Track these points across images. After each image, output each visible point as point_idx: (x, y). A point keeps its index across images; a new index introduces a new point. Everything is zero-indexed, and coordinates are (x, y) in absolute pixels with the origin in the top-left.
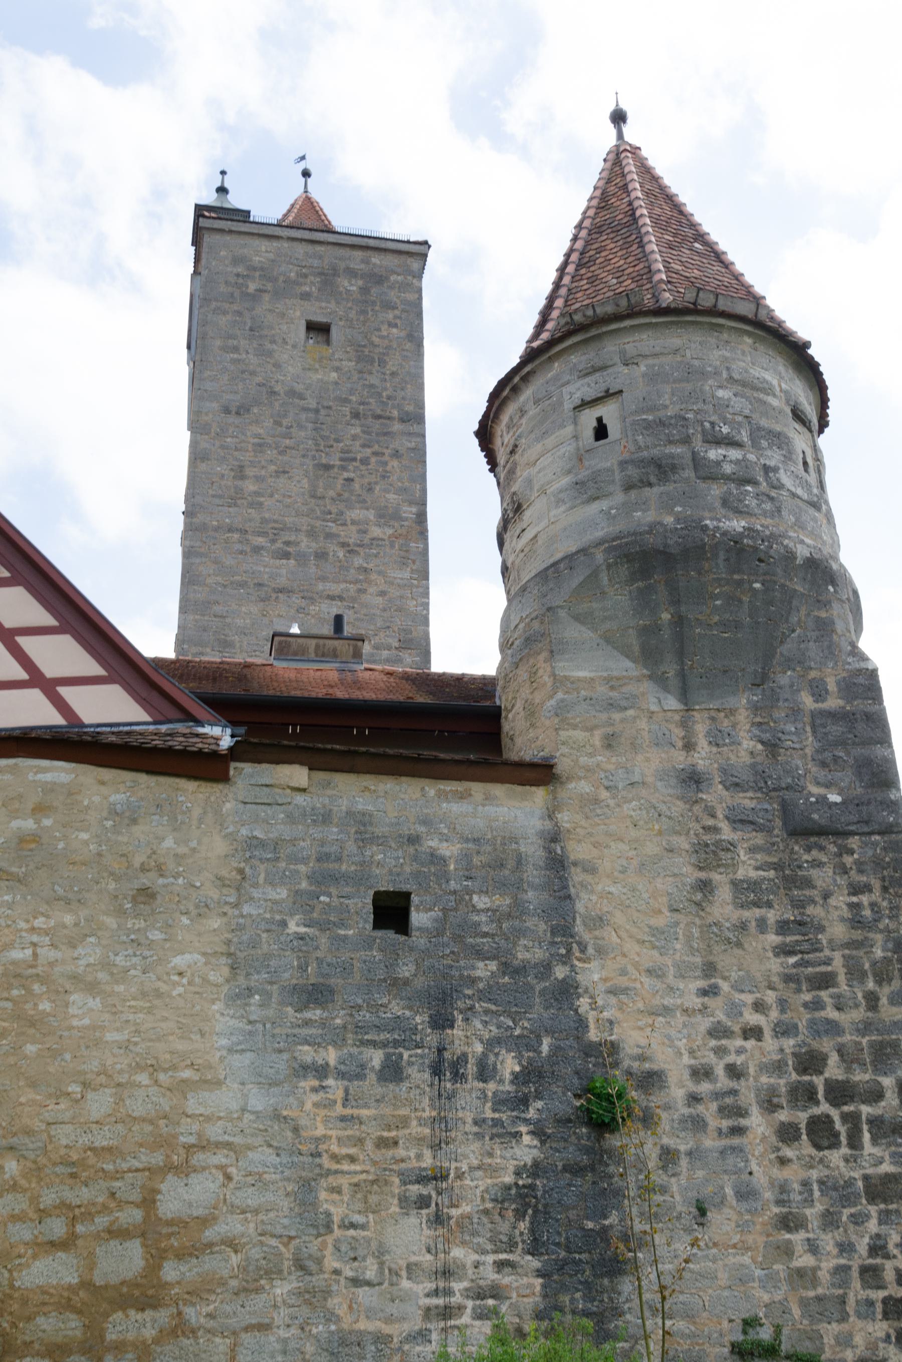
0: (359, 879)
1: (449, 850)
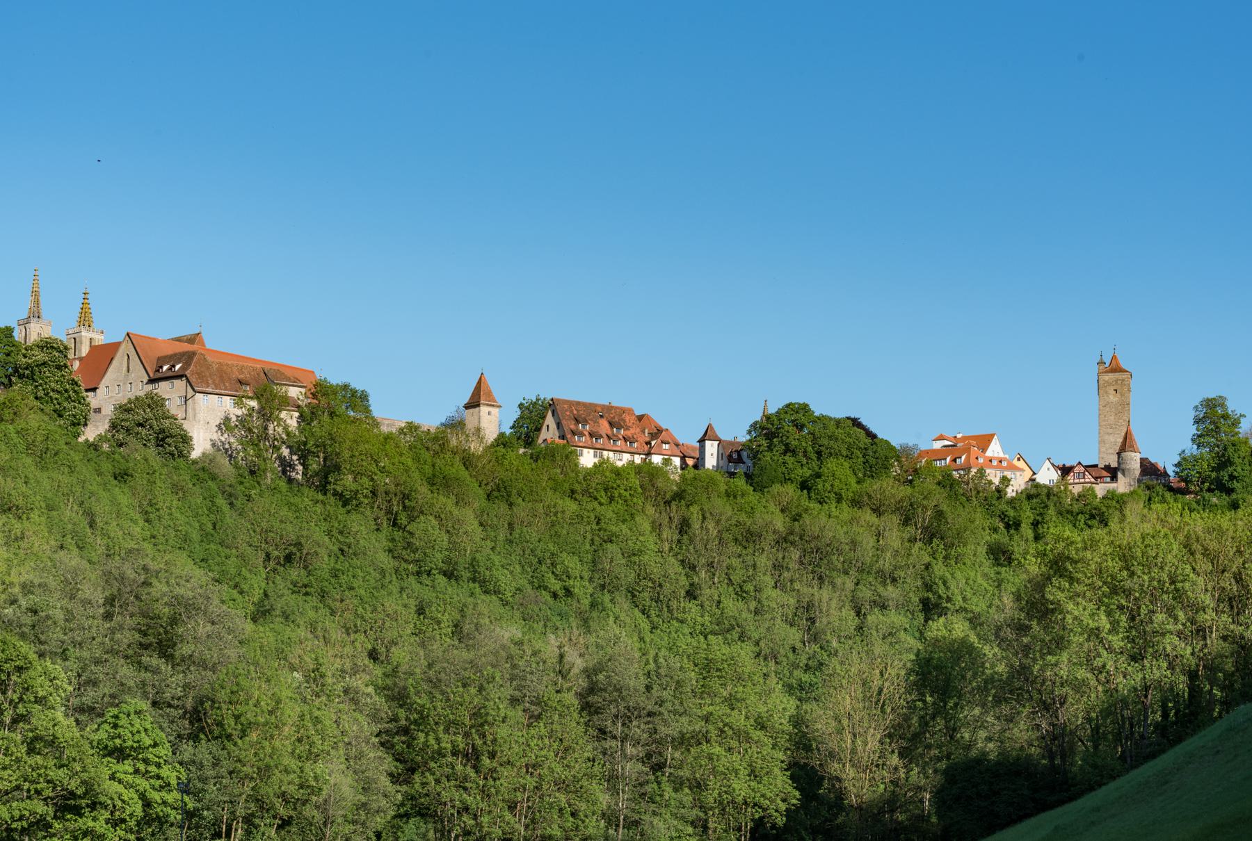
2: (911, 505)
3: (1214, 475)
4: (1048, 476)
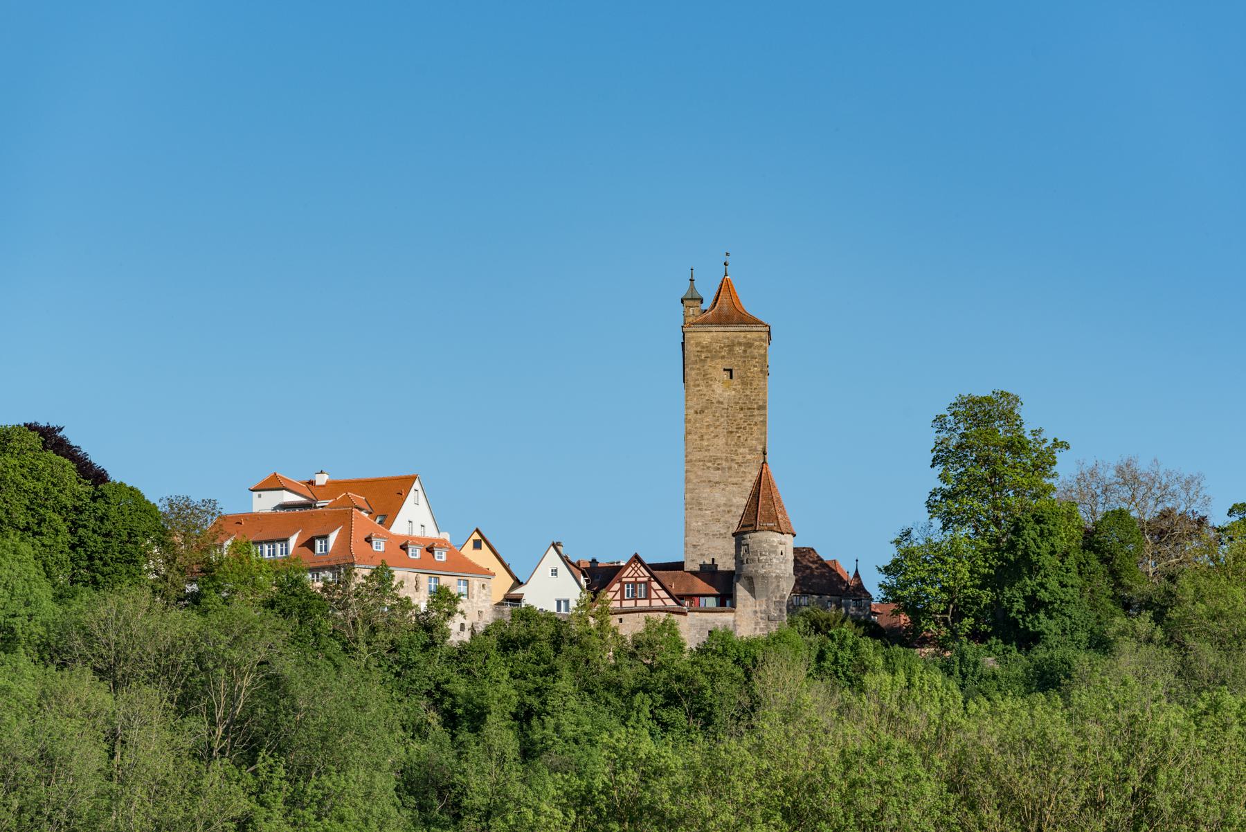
2: (199, 660)
3: (986, 596)
4: (552, 590)
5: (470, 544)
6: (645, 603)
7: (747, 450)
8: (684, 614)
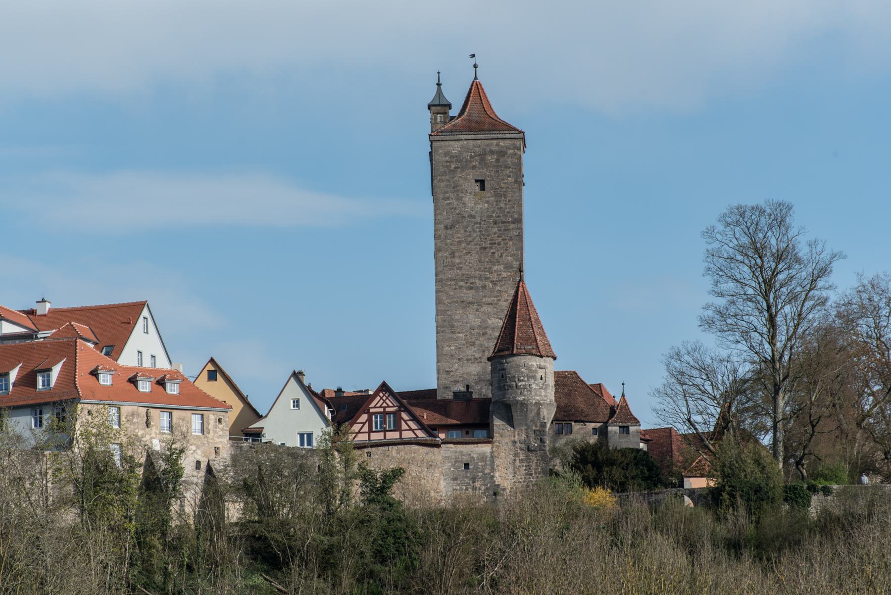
0: (461, 461)
1: (475, 456)
5: (205, 374)
6: (395, 435)
7: (502, 267)
8: (438, 446)
